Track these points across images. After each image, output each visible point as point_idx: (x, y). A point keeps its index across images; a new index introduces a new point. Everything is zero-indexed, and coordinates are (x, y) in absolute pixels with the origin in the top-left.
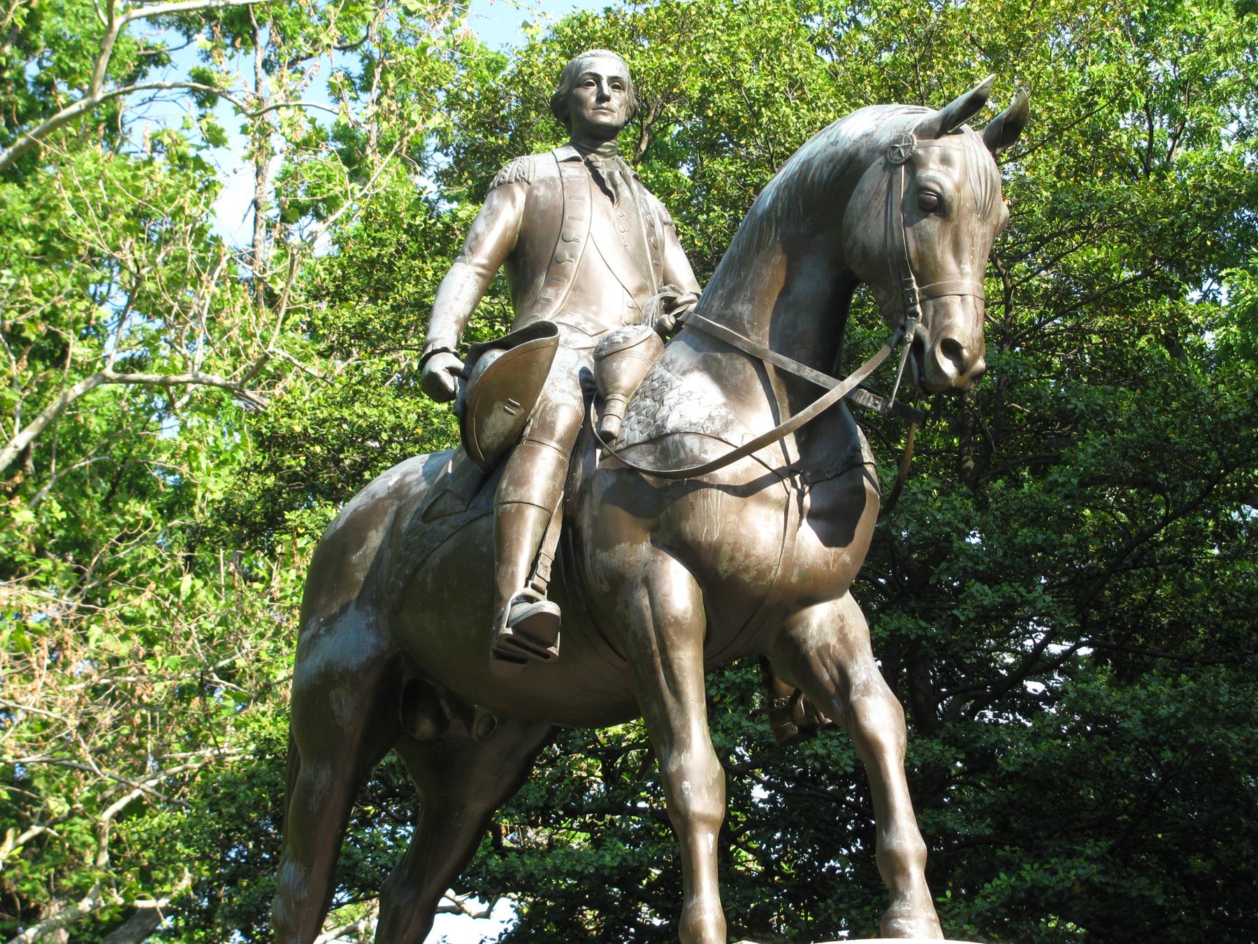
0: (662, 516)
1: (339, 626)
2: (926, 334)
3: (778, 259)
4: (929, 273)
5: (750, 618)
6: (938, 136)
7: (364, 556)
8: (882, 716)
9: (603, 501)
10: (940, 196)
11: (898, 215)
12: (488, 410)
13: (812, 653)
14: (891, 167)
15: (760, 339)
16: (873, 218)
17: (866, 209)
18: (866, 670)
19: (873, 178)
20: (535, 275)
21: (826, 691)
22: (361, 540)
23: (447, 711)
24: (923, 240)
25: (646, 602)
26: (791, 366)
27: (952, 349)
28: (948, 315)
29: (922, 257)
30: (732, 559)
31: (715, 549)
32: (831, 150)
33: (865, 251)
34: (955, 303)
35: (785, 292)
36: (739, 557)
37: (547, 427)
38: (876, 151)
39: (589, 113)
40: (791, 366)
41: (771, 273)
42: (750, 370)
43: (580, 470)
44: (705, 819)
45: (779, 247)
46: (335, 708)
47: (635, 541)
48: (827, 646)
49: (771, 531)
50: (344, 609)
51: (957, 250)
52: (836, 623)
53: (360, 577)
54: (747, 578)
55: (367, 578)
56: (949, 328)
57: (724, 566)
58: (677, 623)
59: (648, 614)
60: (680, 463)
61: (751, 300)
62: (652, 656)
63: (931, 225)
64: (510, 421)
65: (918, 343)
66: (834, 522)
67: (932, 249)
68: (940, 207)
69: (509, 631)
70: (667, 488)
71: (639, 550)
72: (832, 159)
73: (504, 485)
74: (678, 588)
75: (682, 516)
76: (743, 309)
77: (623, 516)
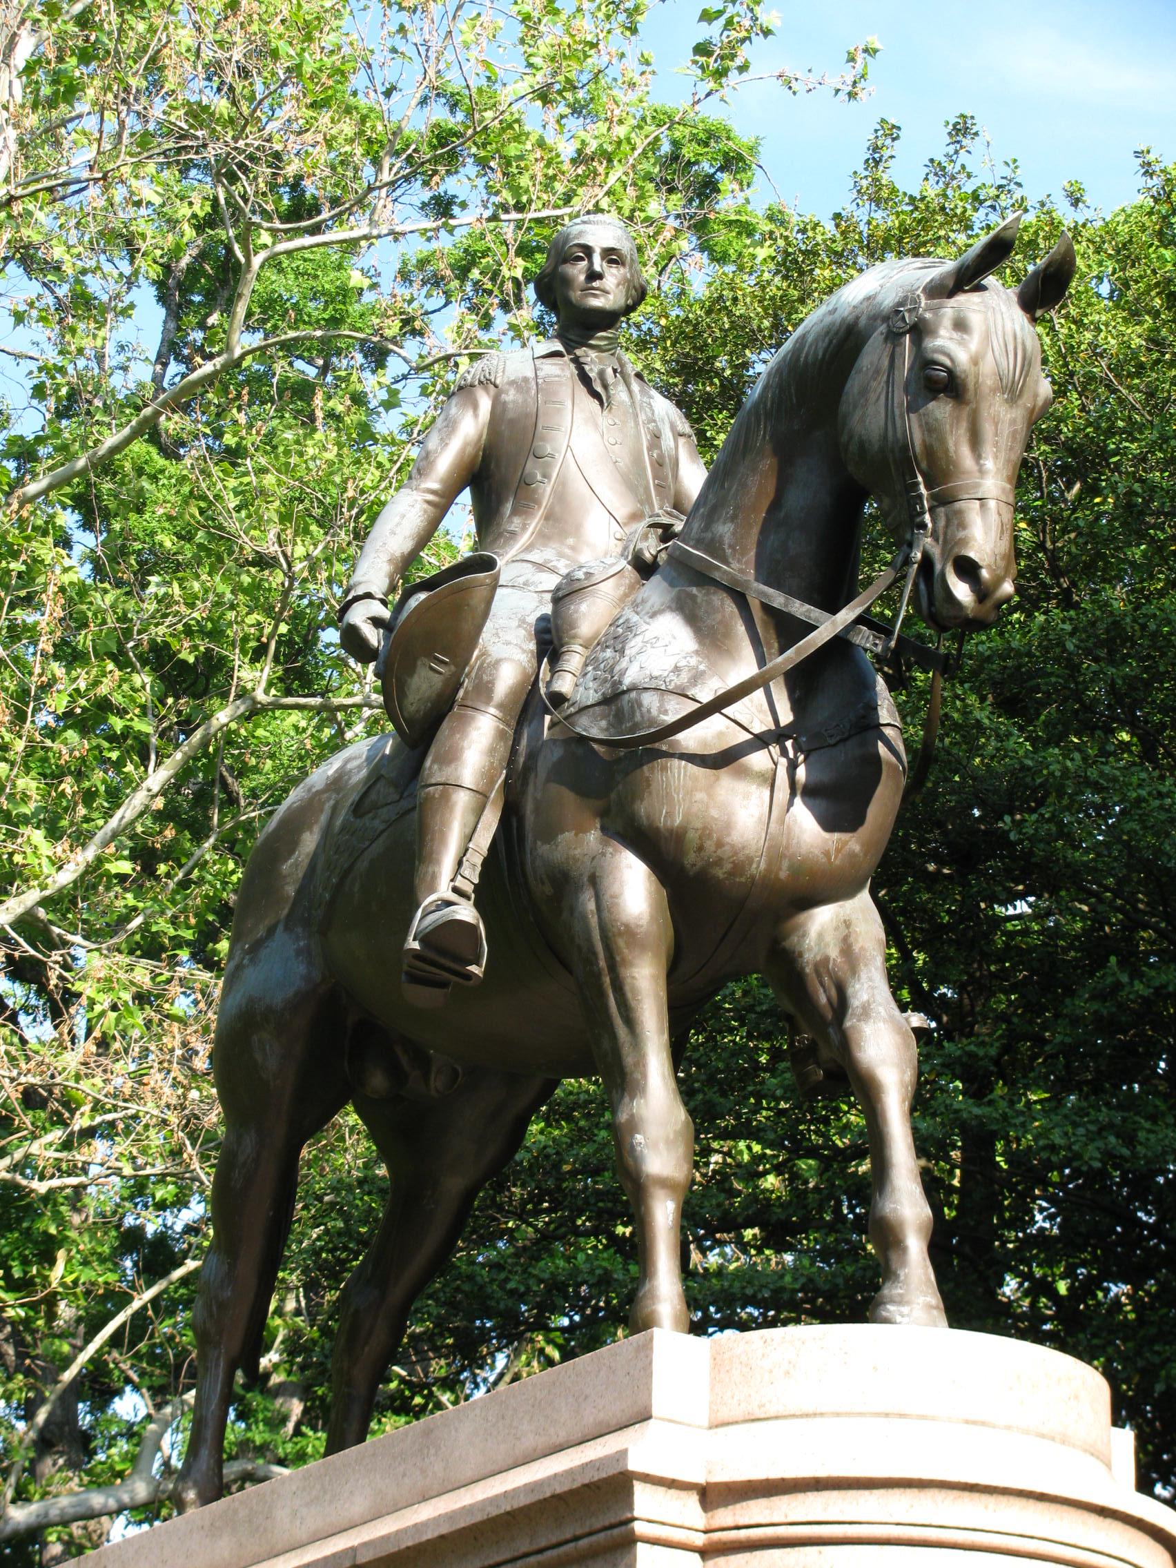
0: (613, 796)
1: (263, 953)
2: (936, 552)
3: (768, 464)
4: (940, 472)
5: (731, 928)
6: (951, 294)
7: (296, 865)
8: (885, 1043)
9: (548, 780)
10: (950, 372)
11: (901, 399)
12: (411, 669)
13: (808, 970)
14: (893, 337)
15: (741, 567)
17: (864, 392)
18: (871, 989)
19: (873, 354)
20: (500, 502)
21: (822, 1017)
22: (293, 844)
23: (404, 1060)
24: (931, 429)
25: (591, 906)
26: (778, 599)
27: (968, 569)
28: (962, 525)
29: (929, 451)
30: (701, 848)
31: (678, 836)
32: (829, 319)
33: (862, 446)
34: (972, 510)
35: (775, 505)
36: (710, 845)
37: (484, 690)
39: (575, 295)
40: (778, 599)
42: (730, 607)
43: (524, 742)
44: (664, 1183)
45: (768, 448)
46: (258, 1057)
47: (581, 829)
48: (826, 959)
49: (756, 813)
50: (271, 931)
51: (975, 441)
53: (291, 890)
54: (720, 873)
55: (299, 892)
56: (964, 542)
57: (691, 859)
58: (629, 932)
59: (594, 921)
61: (733, 518)
62: (598, 976)
63: (941, 409)
64: (437, 681)
66: (839, 802)
67: (942, 441)
68: (947, 385)
69: (416, 945)
70: (619, 760)
71: (586, 841)
73: (428, 763)
74: (633, 888)
75: (635, 795)
77: (569, 798)
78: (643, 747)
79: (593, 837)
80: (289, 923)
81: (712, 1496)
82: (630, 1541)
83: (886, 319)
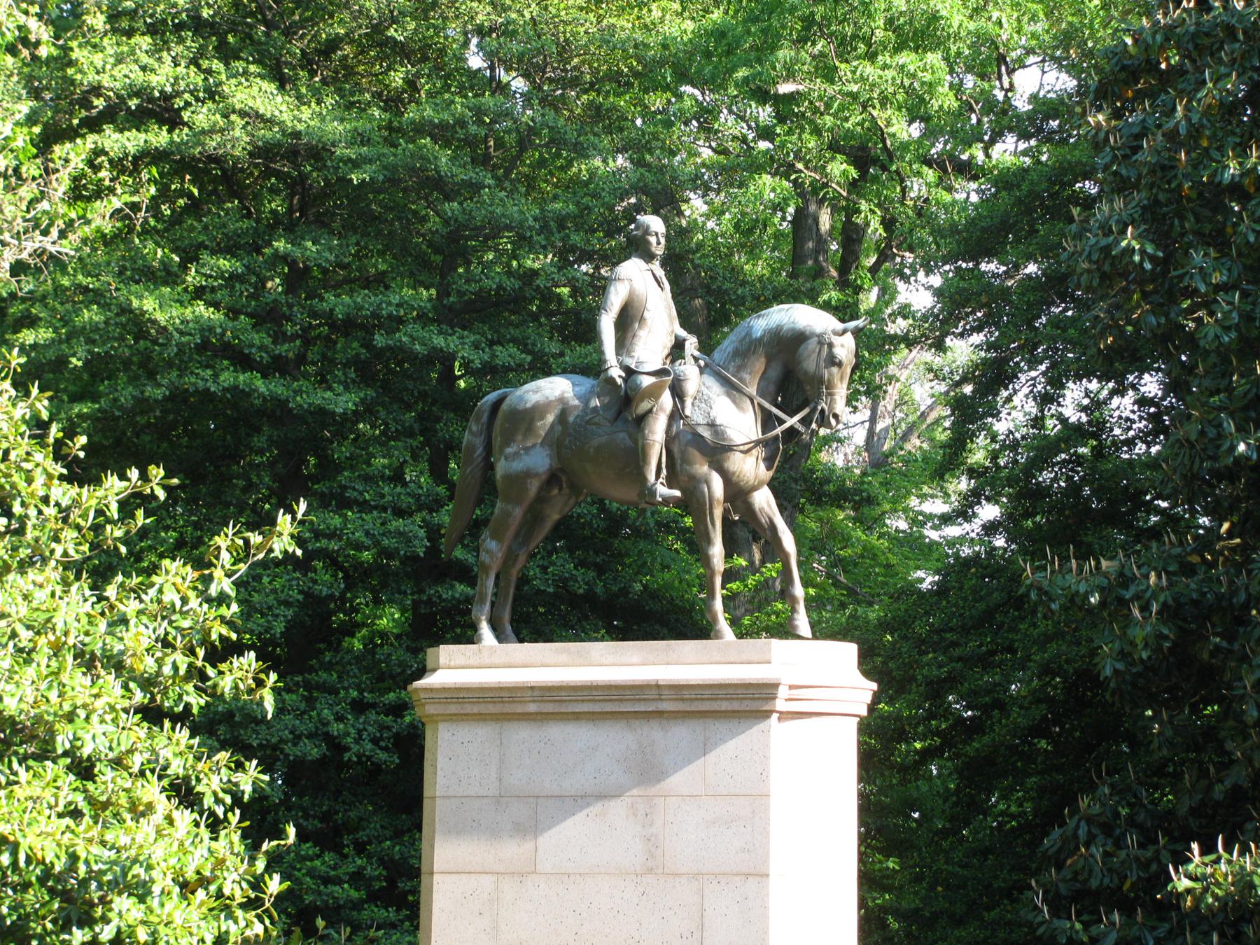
1: (532, 452)
5: (738, 494)
11: (822, 364)
12: (642, 401)
14: (821, 343)
15: (752, 390)
16: (810, 361)
17: (809, 356)
20: (632, 323)
22: (542, 418)
24: (830, 374)
26: (767, 405)
29: (829, 381)
31: (734, 473)
33: (806, 373)
34: (837, 397)
35: (764, 373)
37: (662, 409)
38: (813, 334)
40: (767, 405)
41: (759, 364)
42: (748, 402)
49: (750, 467)
50: (534, 446)
52: (764, 500)
53: (543, 433)
57: (735, 478)
60: (724, 440)
63: (835, 370)
65: (823, 411)
66: (769, 461)
68: (840, 364)
71: (703, 468)
72: (793, 330)
74: (717, 485)
75: (725, 460)
76: (747, 377)
77: (696, 453)
78: (730, 449)
79: (705, 468)
80: (542, 444)
81: (791, 687)
82: (775, 698)
83: (818, 336)
